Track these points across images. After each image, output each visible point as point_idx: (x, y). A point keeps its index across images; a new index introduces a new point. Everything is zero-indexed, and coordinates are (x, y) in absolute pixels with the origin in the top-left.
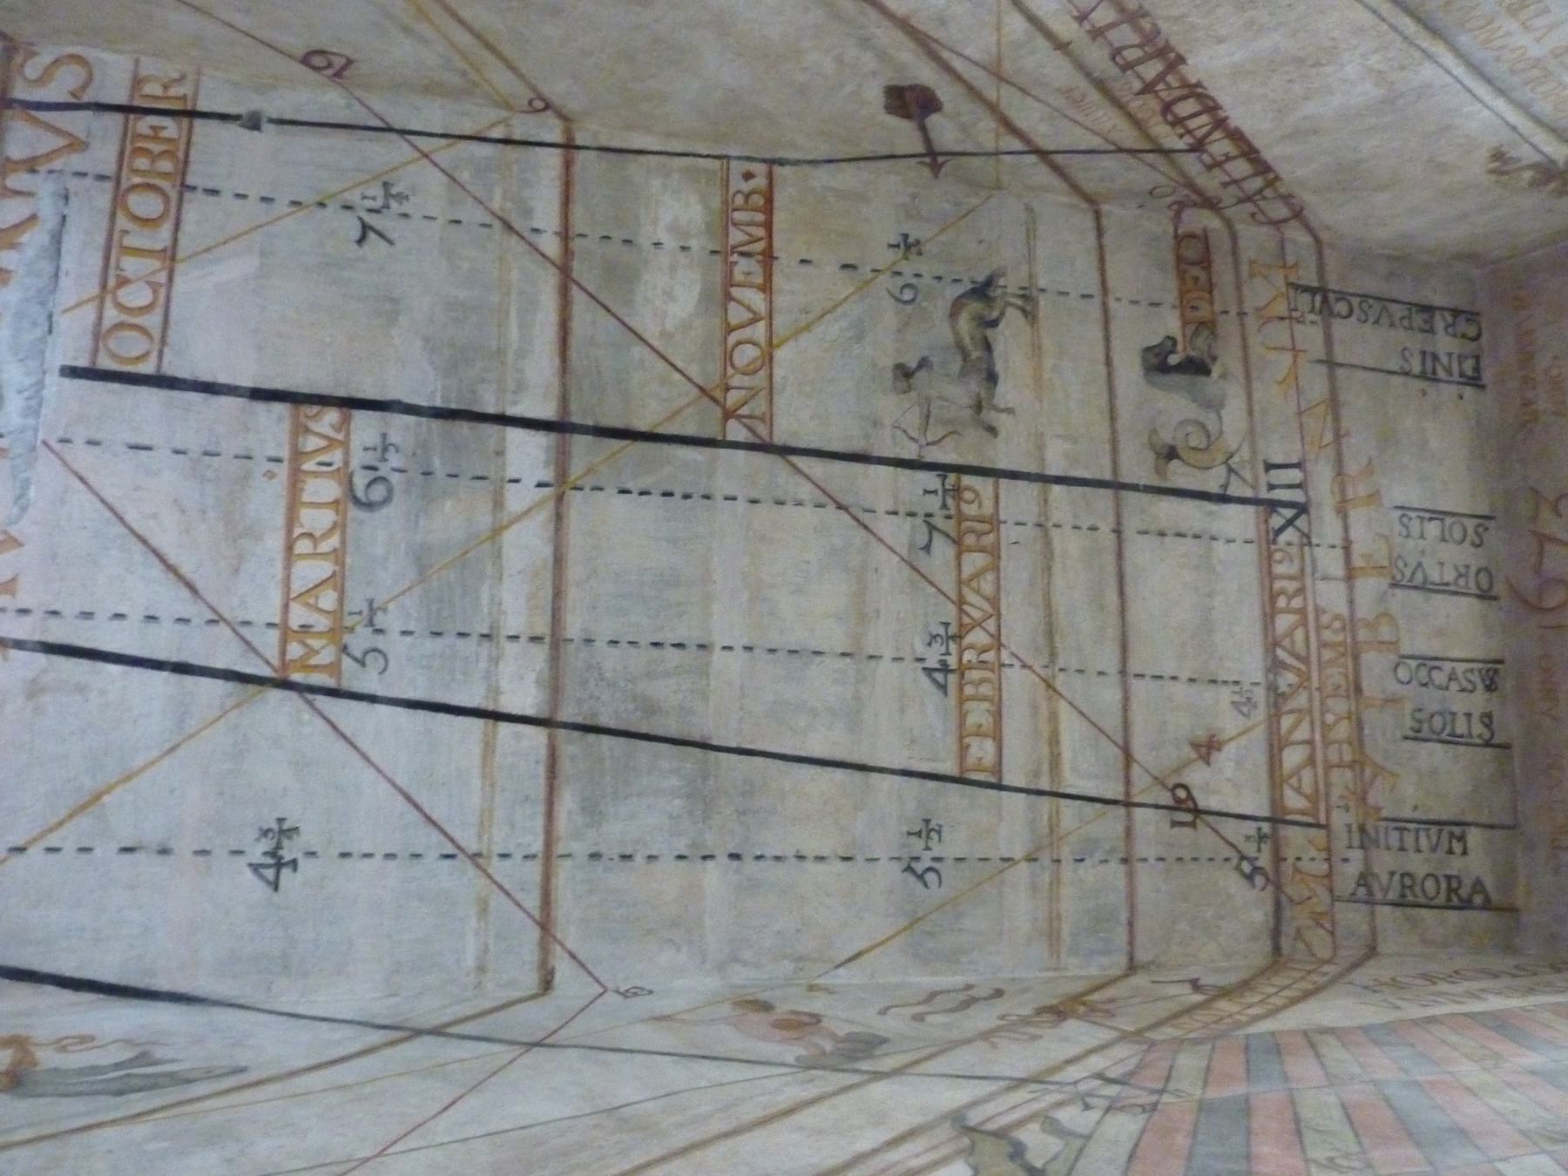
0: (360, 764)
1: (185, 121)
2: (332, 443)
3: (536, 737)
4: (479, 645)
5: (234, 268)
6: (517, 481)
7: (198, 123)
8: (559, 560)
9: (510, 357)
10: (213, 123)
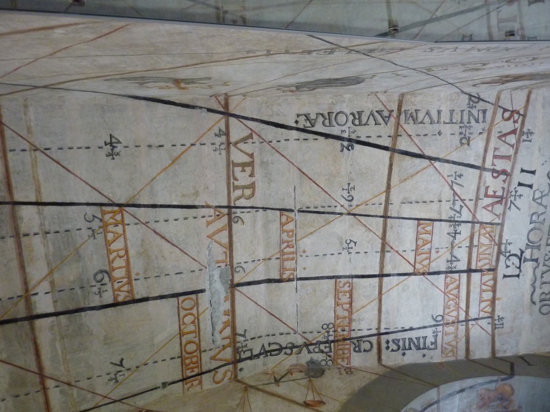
0: (88, 181)
1: (185, 377)
2: (119, 290)
3: (18, 197)
4: (50, 230)
5: (161, 337)
6: (46, 293)
7: (181, 378)
8: (22, 267)
9: (58, 338)
10: (177, 379)
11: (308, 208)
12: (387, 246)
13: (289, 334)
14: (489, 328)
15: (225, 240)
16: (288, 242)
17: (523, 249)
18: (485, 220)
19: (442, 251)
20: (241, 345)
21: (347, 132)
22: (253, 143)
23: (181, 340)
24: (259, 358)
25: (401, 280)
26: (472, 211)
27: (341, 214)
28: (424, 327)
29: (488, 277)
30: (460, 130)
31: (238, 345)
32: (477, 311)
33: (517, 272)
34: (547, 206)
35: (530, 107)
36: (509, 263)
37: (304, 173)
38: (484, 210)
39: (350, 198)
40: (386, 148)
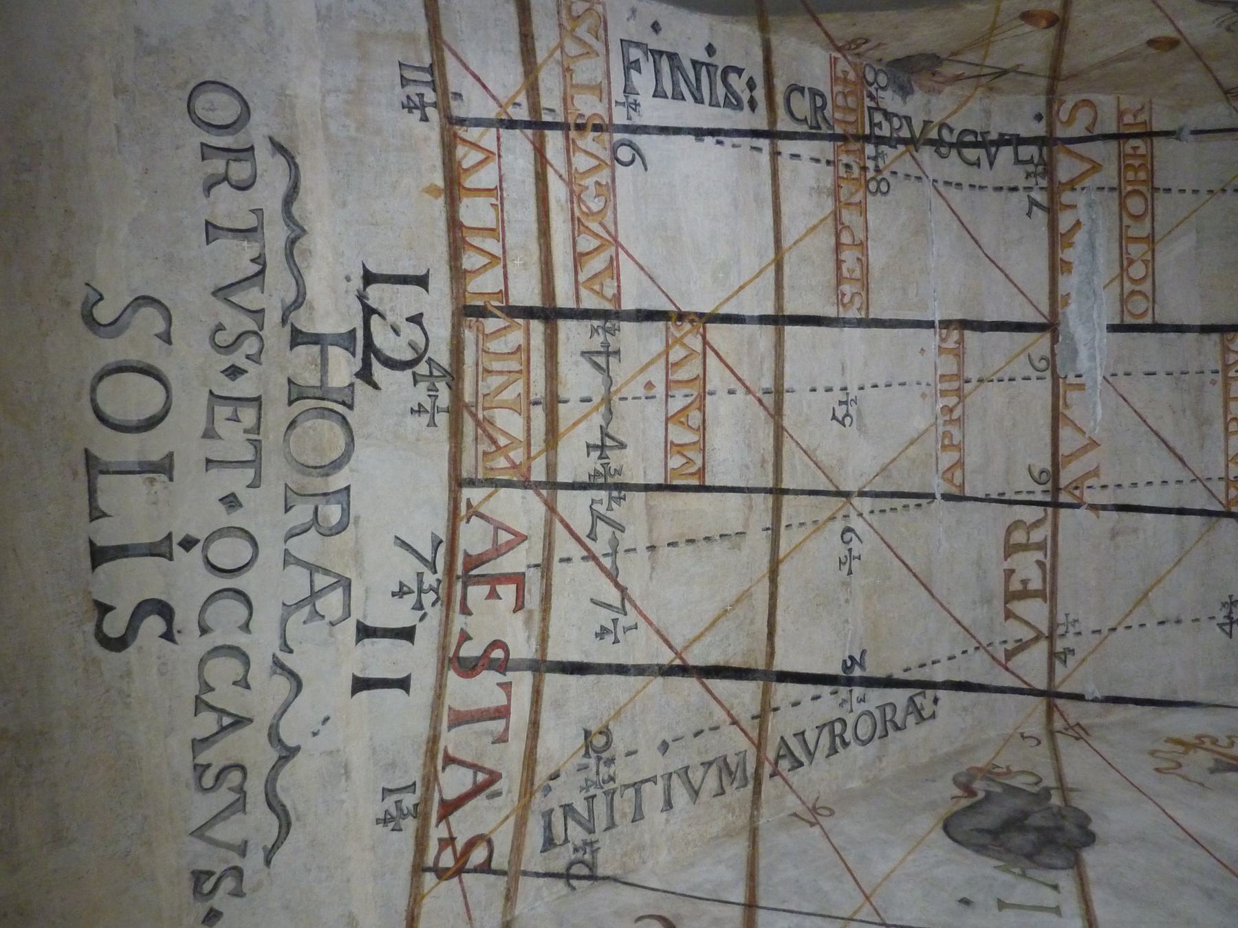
7: (1155, 140)
11: (919, 505)
13: (947, 183)
14: (456, 79)
15: (1065, 432)
16: (951, 421)
17: (361, 388)
18: (517, 493)
19: (637, 388)
20: (1039, 180)
21: (854, 700)
22: (1005, 642)
23: (1153, 228)
24: (1001, 135)
26: (558, 526)
27: (862, 494)
28: (664, 130)
29: (484, 284)
30: (613, 768)
32: (507, 158)
33: (375, 293)
34: (285, 563)
35: (402, 903)
36: (412, 333)
37: (926, 588)
38: (524, 531)
39: (848, 536)
40: (784, 677)
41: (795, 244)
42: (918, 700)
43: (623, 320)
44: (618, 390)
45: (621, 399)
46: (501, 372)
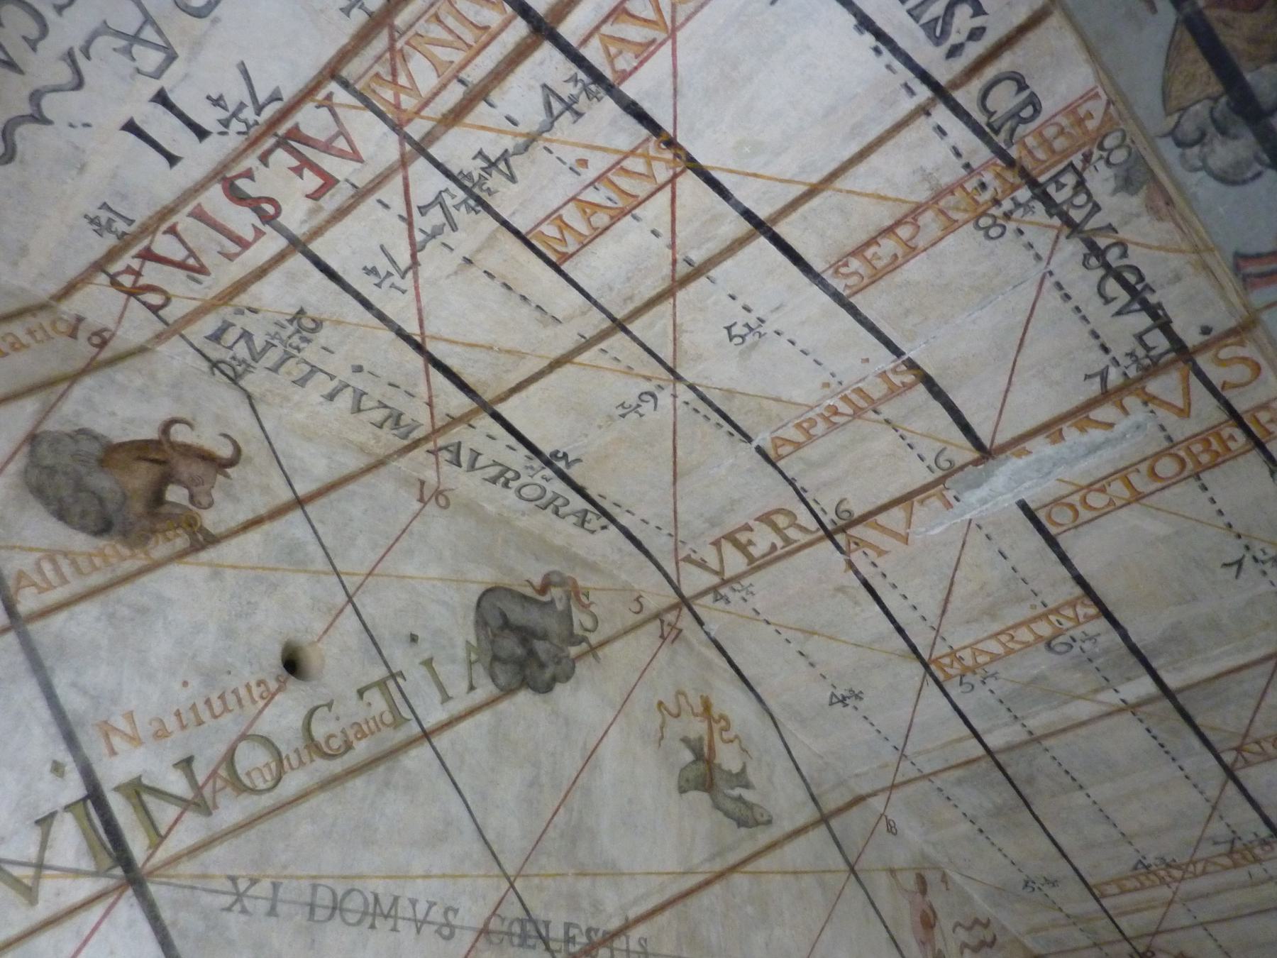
11: (732, 434)
12: (677, 276)
15: (898, 513)
16: (827, 419)
19: (571, 156)
20: (1134, 367)
23: (1152, 493)
24: (1160, 305)
25: (735, 178)
27: (692, 387)
30: (302, 345)
31: (1133, 372)
38: (363, 155)
40: (497, 417)
41: (849, 192)
42: (590, 516)
43: (612, 96)
44: (550, 141)
45: (545, 148)
46: (451, 31)
